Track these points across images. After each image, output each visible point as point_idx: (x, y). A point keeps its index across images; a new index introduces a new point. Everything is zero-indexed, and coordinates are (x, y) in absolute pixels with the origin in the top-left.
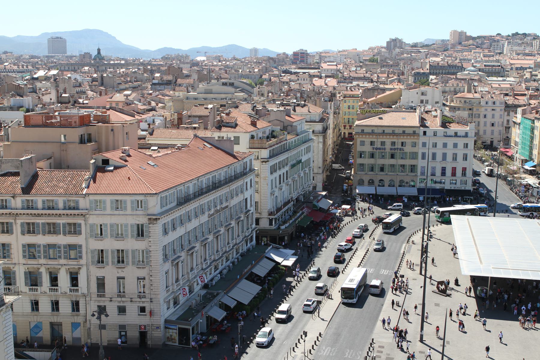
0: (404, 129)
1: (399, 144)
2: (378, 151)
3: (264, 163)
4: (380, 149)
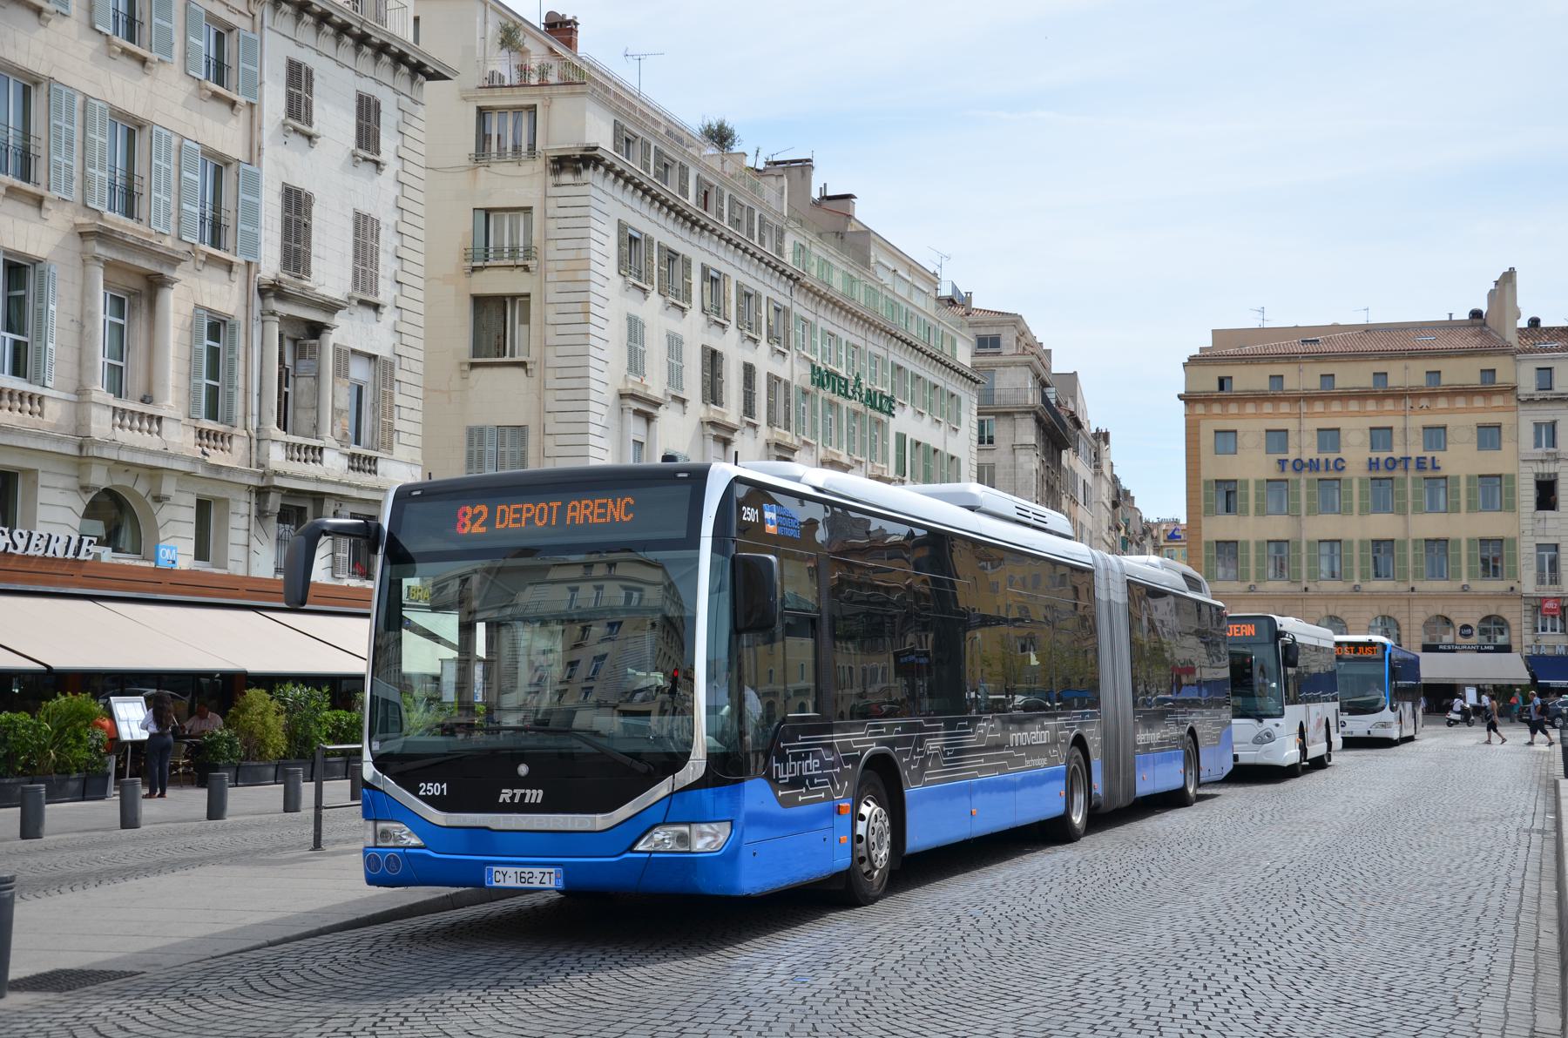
0: (1434, 365)
1: (1412, 437)
2: (1306, 476)
3: (567, 178)
4: (1313, 465)
